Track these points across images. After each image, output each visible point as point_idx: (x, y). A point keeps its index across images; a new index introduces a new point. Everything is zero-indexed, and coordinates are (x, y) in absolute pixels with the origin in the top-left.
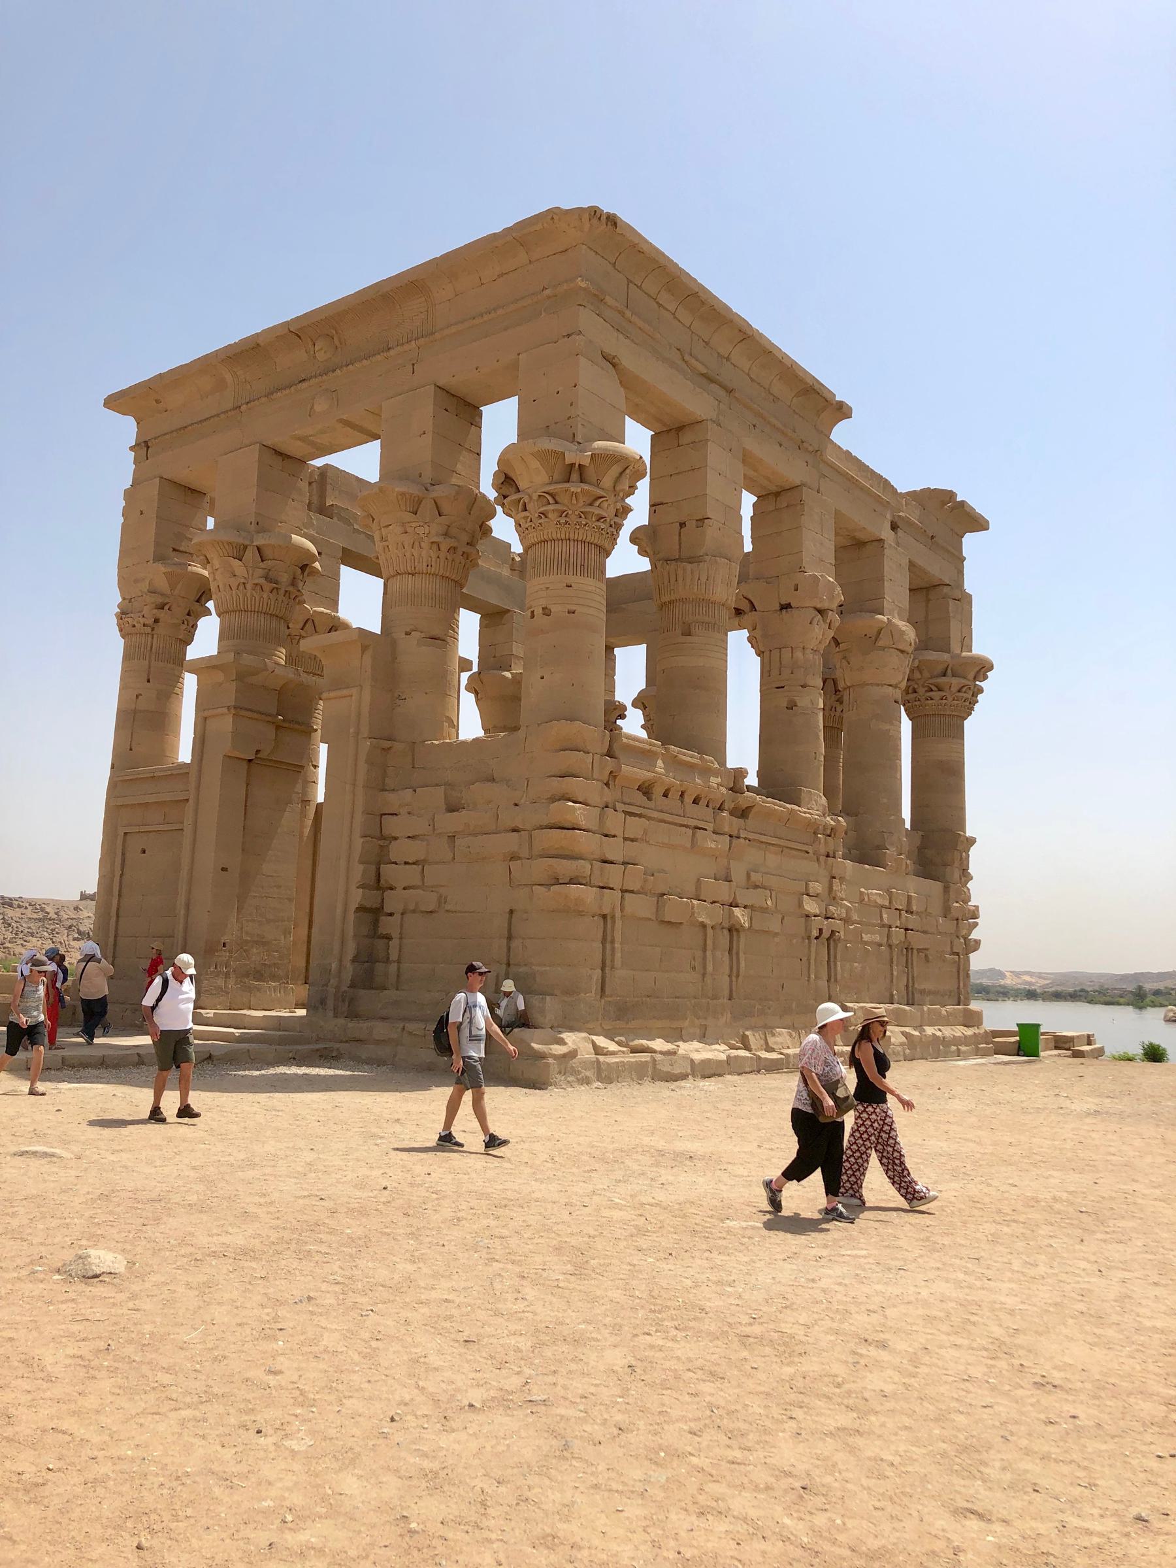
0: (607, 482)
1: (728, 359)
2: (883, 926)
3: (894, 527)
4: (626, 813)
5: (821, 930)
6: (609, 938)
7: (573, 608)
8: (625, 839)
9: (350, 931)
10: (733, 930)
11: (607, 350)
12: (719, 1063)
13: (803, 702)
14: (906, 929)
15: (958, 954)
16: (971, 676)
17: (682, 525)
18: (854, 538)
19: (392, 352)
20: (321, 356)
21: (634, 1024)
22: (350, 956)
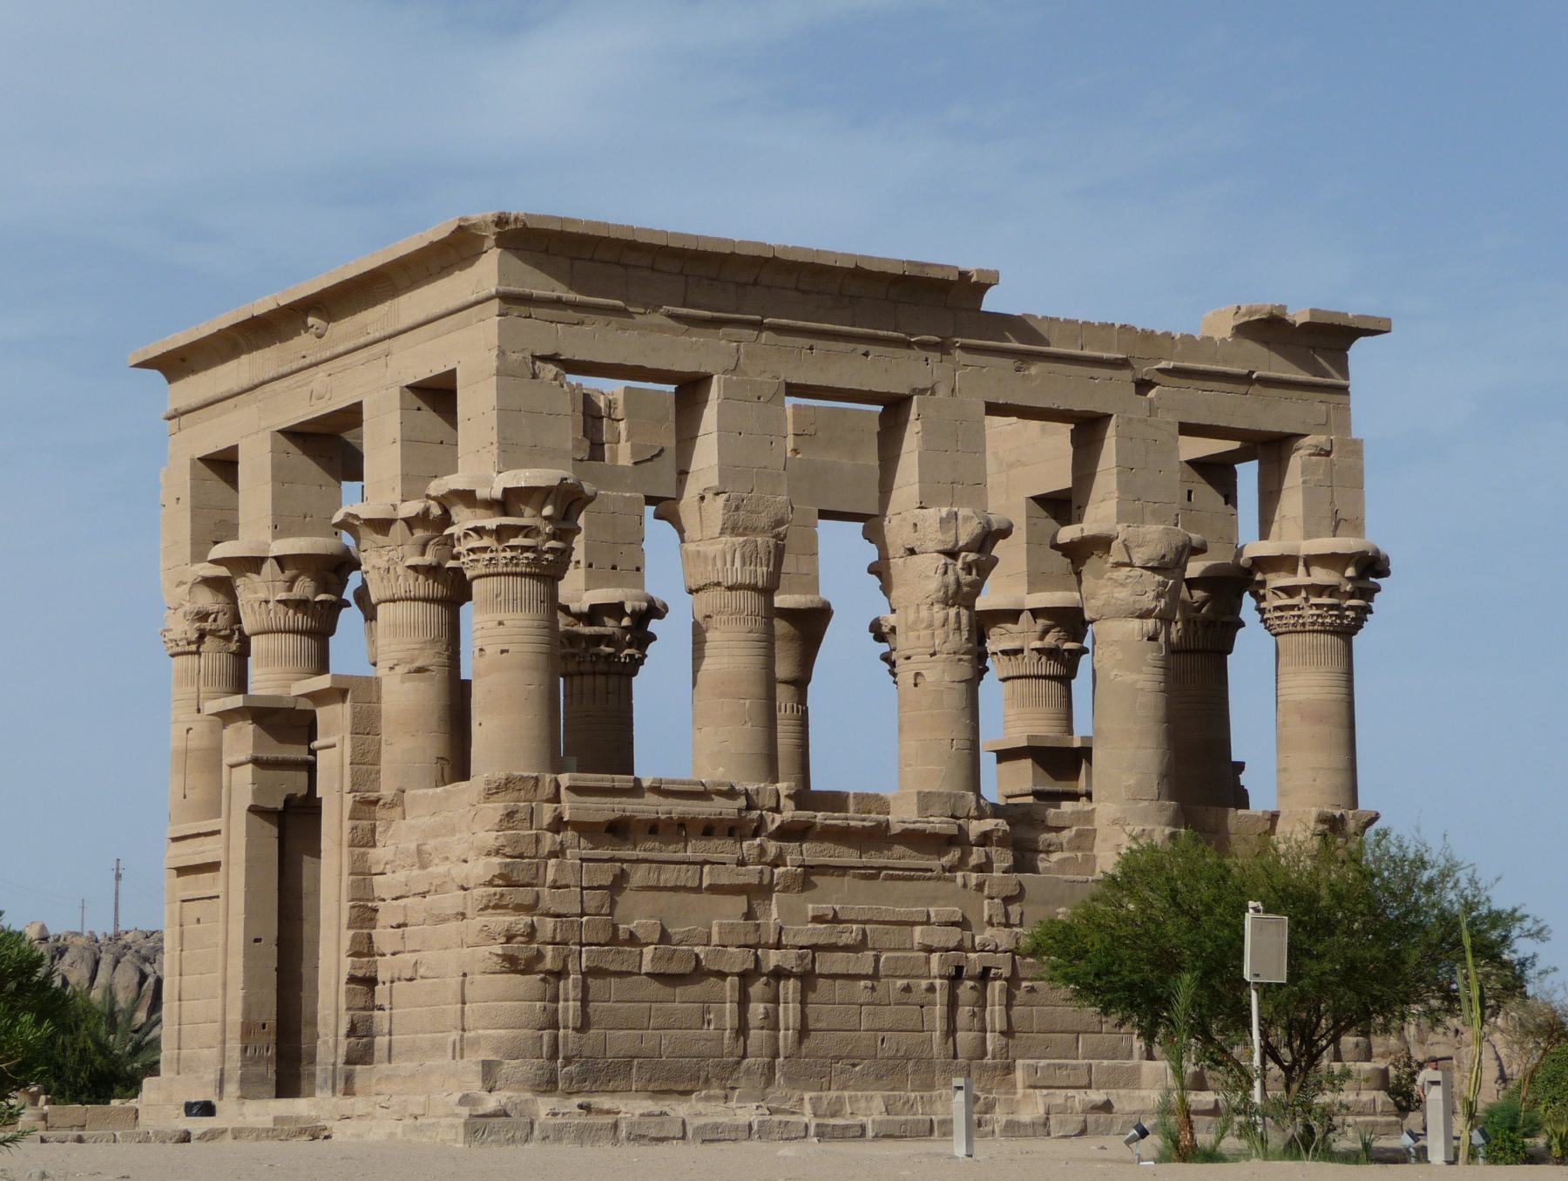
4: (582, 860)
5: (959, 969)
7: (506, 647)
8: (583, 888)
9: (343, 1005)
17: (702, 498)
22: (343, 1030)
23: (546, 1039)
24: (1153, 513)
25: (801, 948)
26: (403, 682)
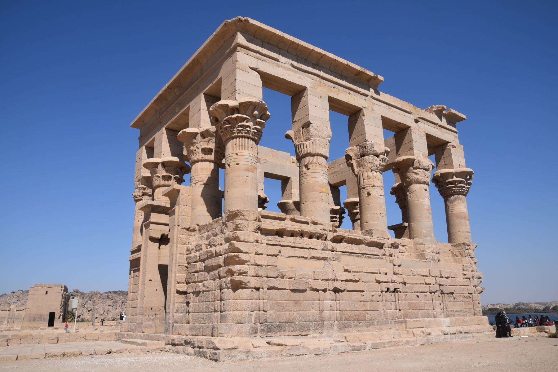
0: (249, 112)
1: (318, 65)
2: (426, 284)
3: (416, 121)
4: (268, 244)
5: (388, 289)
6: (261, 298)
7: (238, 162)
8: (268, 255)
10: (336, 291)
11: (251, 66)
12: (325, 349)
13: (373, 192)
14: (440, 285)
15: (471, 294)
16: (464, 177)
18: (399, 128)
19: (193, 86)
20: (177, 94)
21: (279, 334)
23: (254, 315)
24: (423, 155)
25: (342, 281)
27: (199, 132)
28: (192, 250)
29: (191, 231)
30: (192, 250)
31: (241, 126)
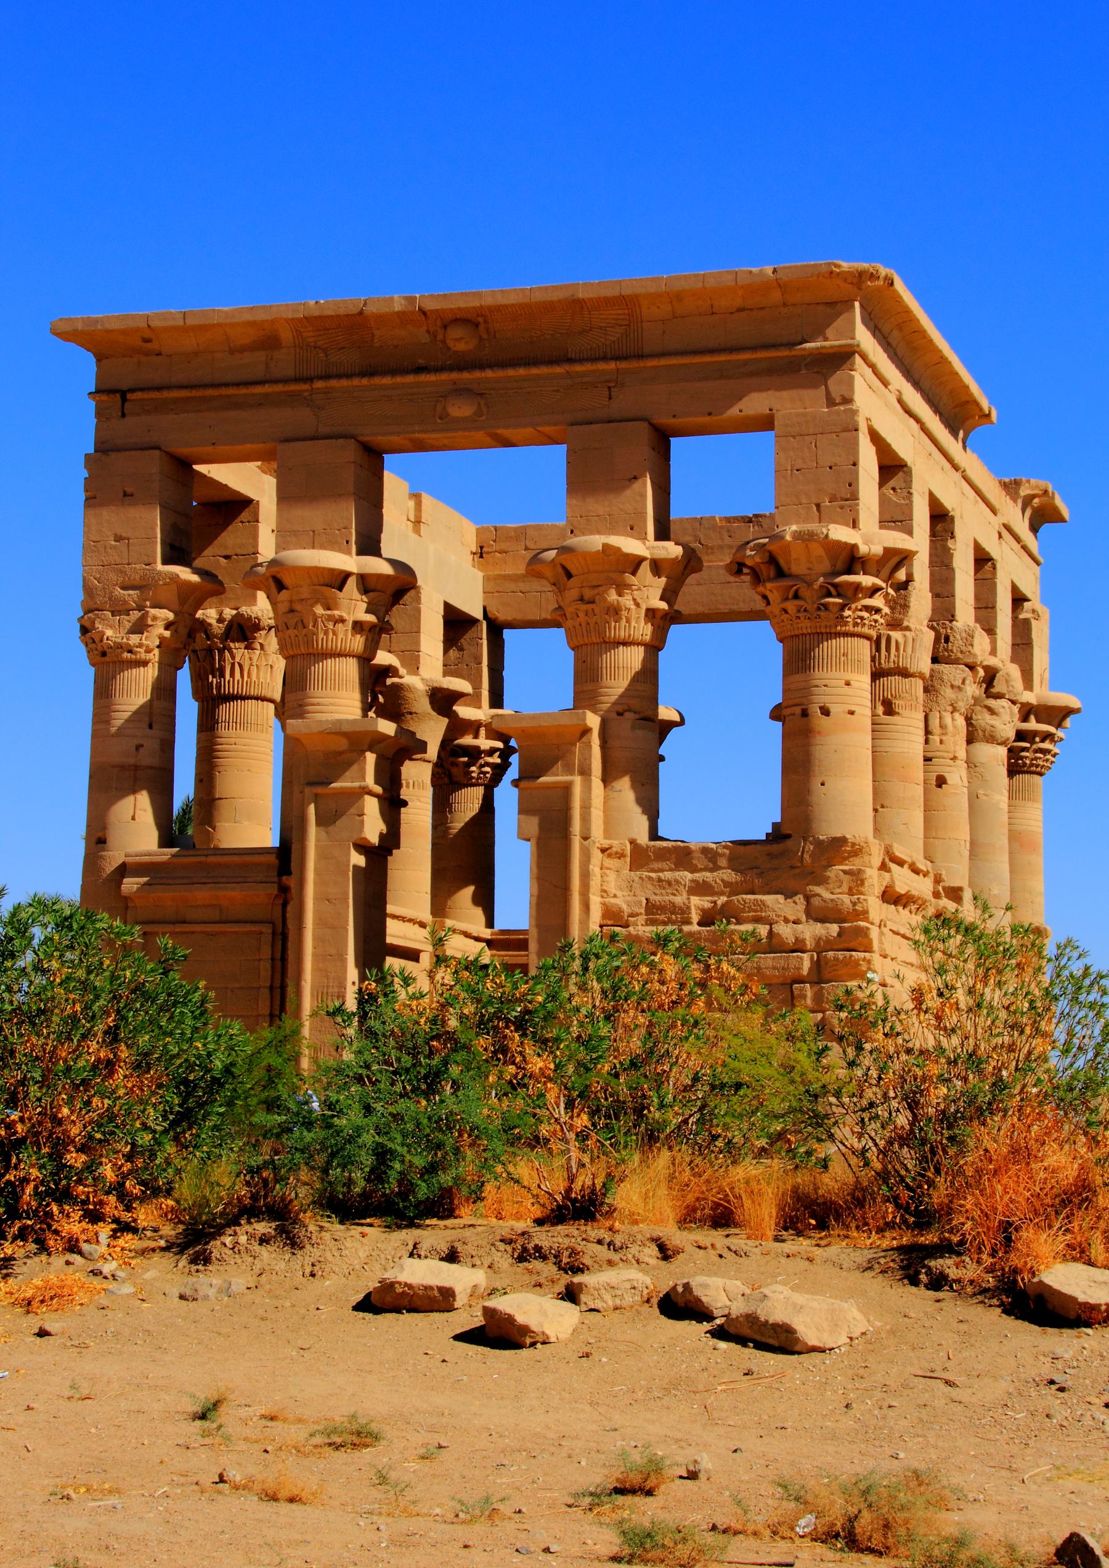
7: (853, 708)
26: (633, 728)
27: (646, 553)
28: (632, 915)
29: (610, 856)
30: (632, 915)
31: (867, 608)
